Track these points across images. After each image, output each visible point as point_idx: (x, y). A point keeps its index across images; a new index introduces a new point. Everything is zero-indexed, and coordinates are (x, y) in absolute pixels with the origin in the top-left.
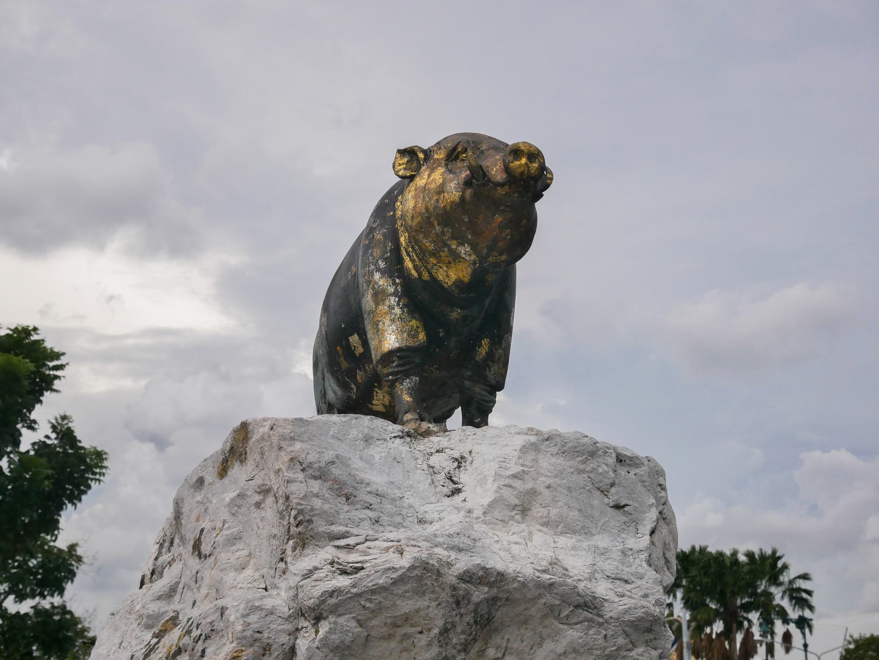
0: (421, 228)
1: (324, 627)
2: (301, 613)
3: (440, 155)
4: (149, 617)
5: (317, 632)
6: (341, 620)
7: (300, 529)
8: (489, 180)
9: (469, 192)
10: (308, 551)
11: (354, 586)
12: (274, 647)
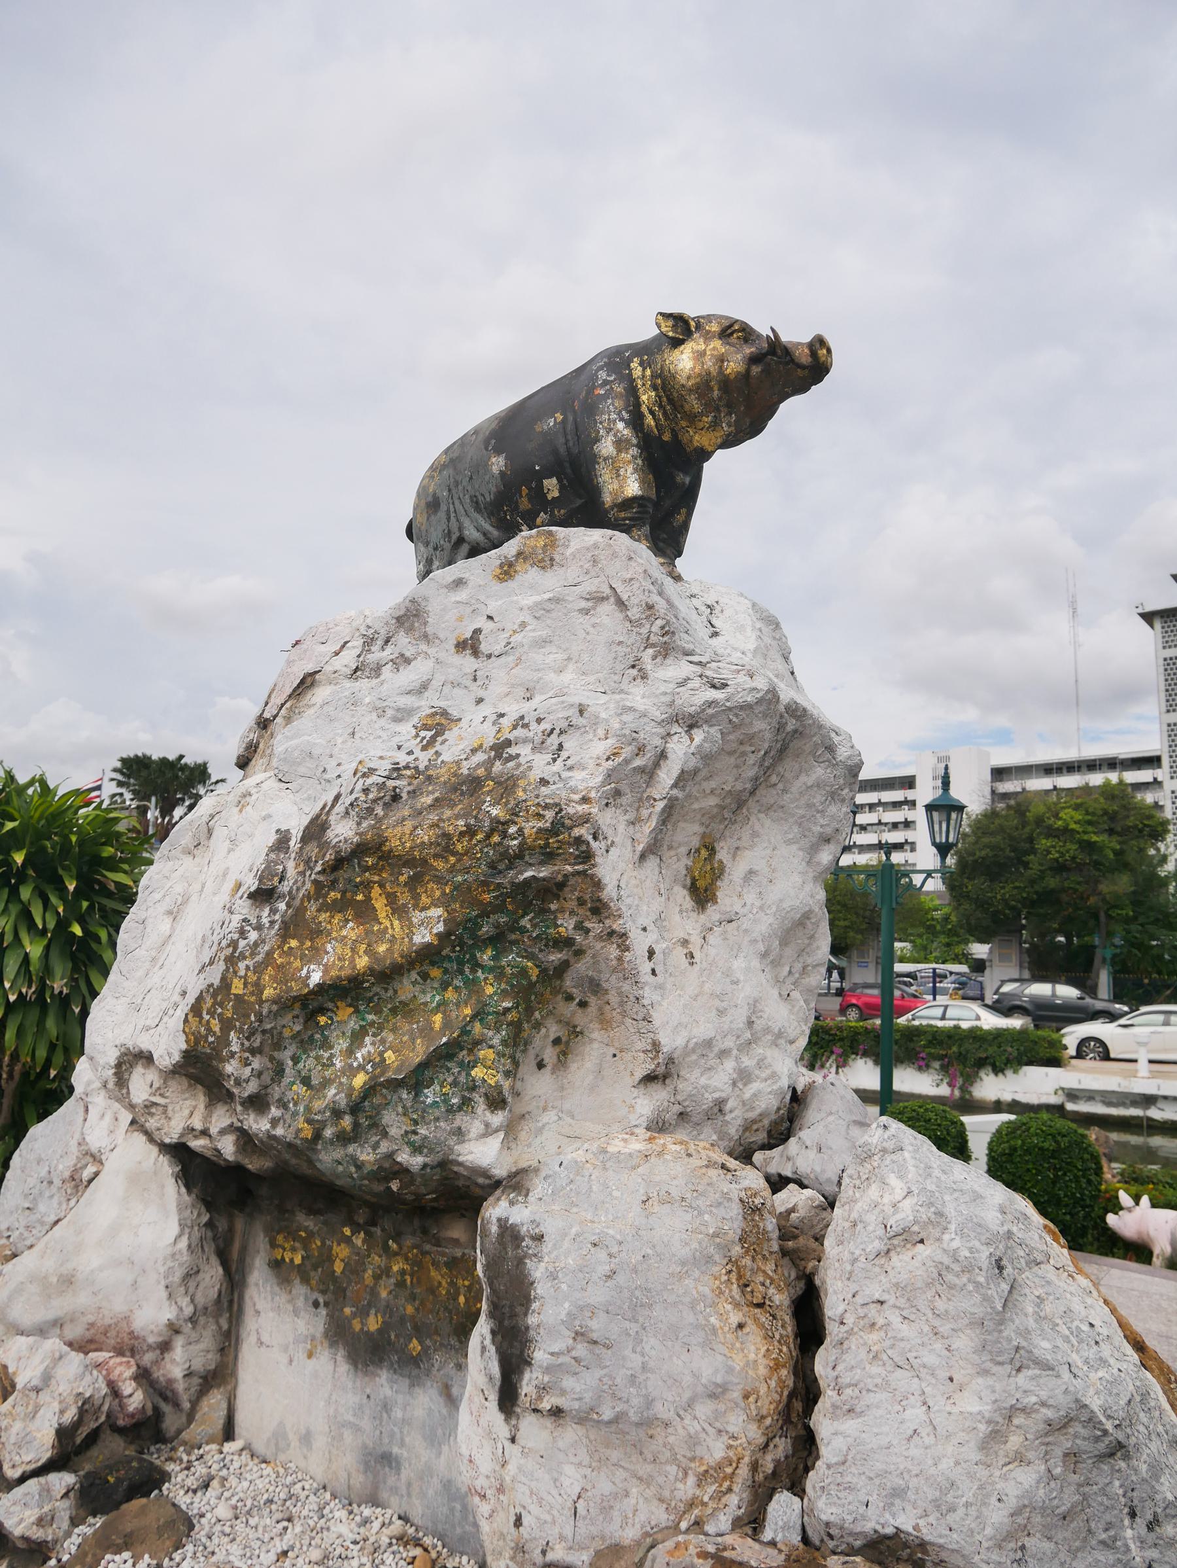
0: (698, 388)
1: (699, 735)
2: (675, 719)
3: (714, 327)
4: (398, 710)
5: (692, 740)
6: (713, 730)
7: (666, 638)
8: (792, 361)
9: (756, 370)
10: (668, 661)
11: (728, 700)
12: (649, 748)
